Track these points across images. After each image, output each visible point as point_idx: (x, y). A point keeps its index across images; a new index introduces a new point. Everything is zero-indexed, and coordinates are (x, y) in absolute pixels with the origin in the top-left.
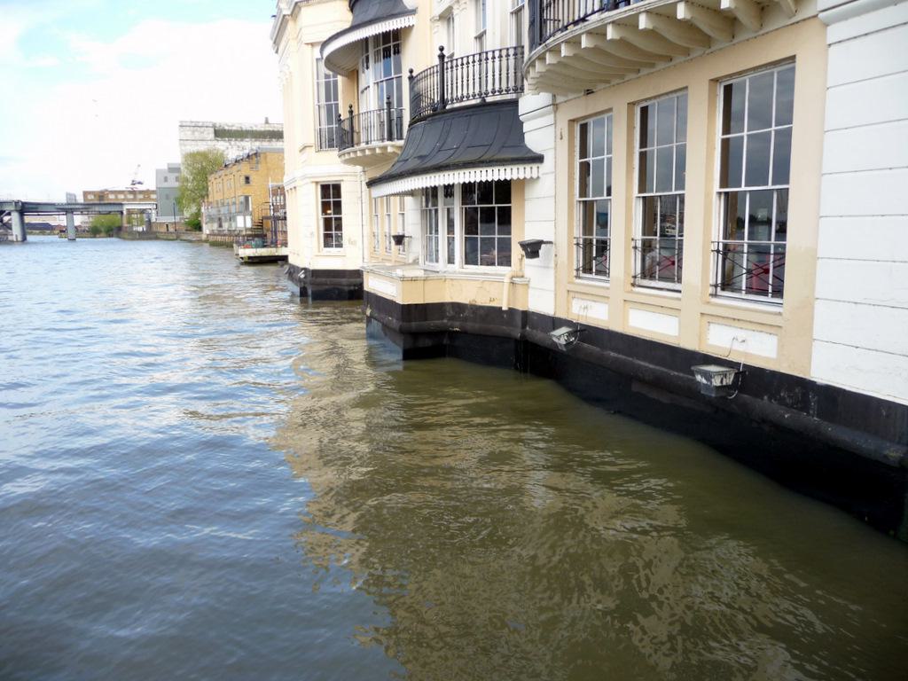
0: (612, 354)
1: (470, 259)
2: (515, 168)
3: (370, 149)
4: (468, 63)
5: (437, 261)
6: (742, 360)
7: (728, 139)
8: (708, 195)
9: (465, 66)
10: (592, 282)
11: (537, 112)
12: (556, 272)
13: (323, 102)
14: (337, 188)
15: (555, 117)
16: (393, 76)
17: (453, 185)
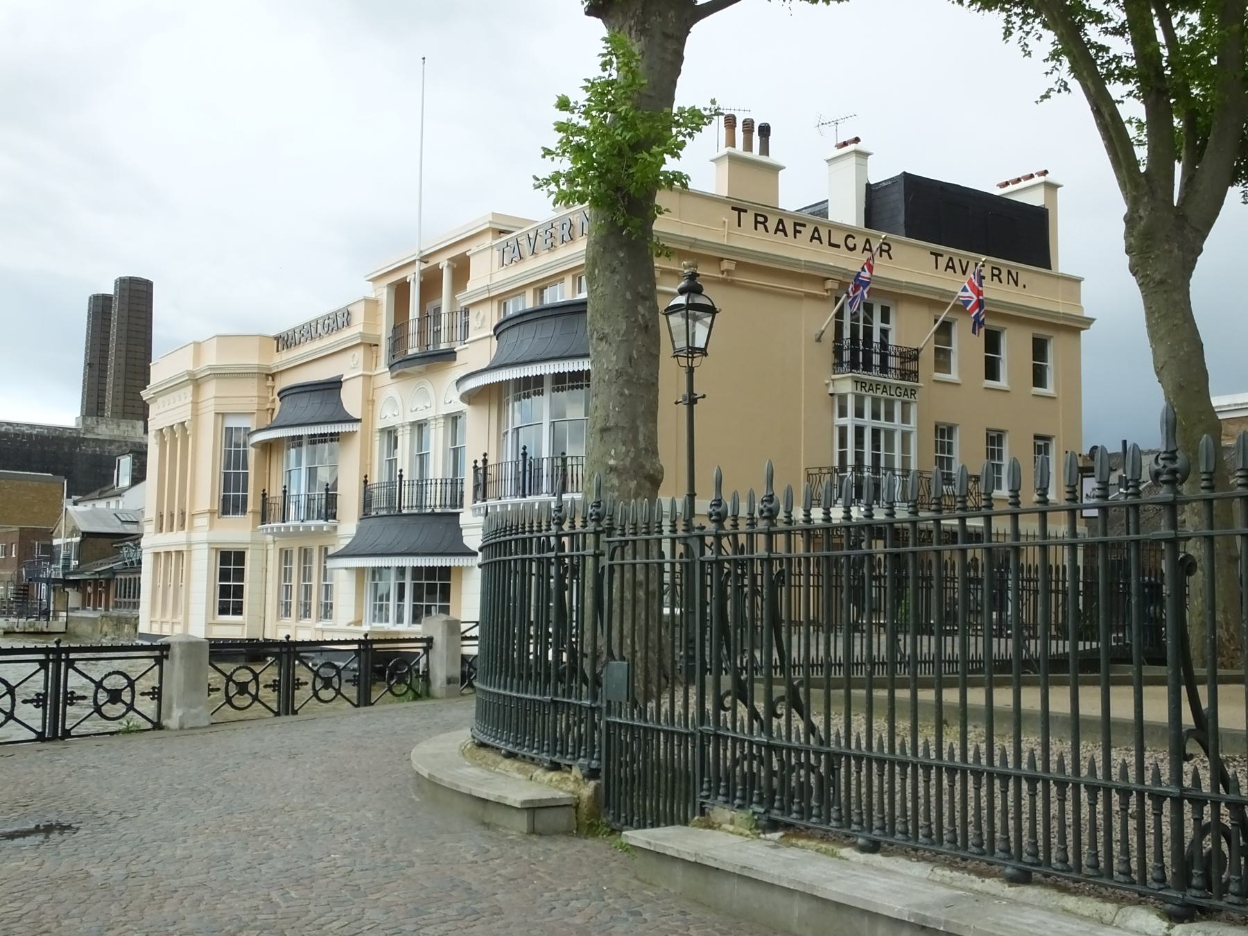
14: (240, 557)
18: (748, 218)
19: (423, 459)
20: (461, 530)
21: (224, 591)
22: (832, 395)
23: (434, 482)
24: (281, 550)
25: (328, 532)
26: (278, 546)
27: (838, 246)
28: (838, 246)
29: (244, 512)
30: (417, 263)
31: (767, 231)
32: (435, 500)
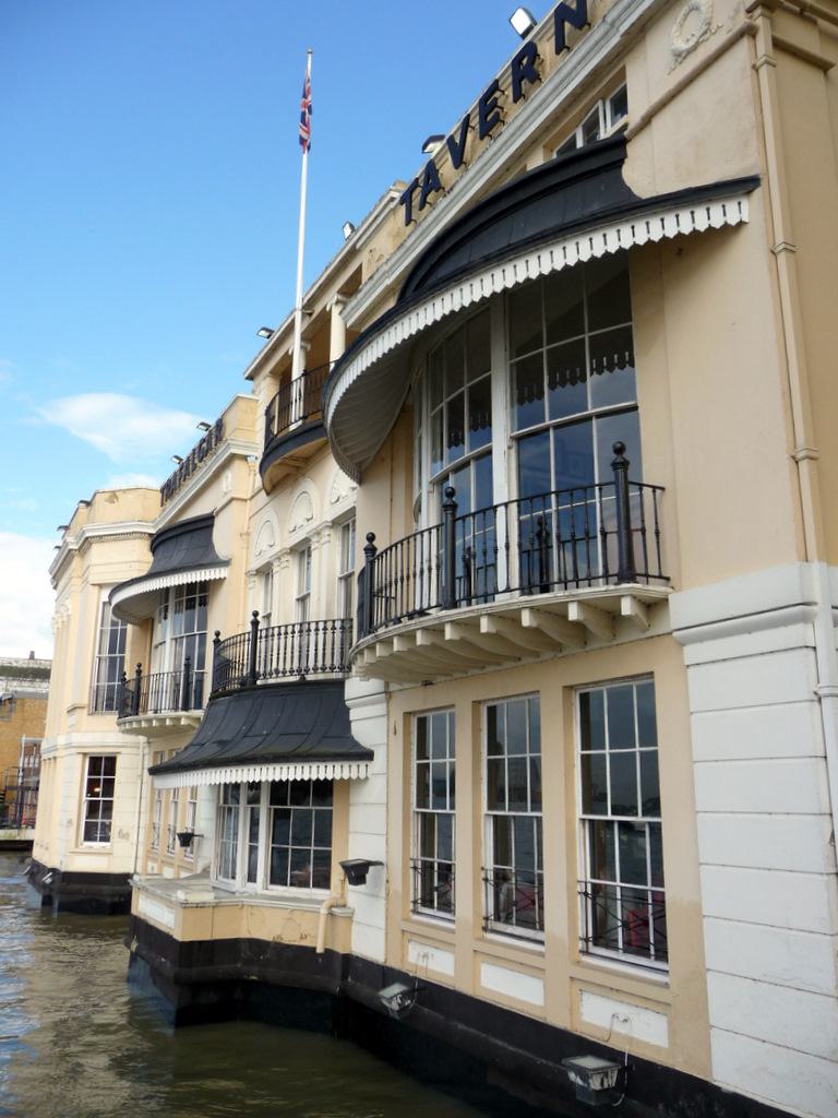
0: (461, 1026)
1: (277, 877)
2: (338, 765)
3: (158, 719)
4: (286, 633)
5: (234, 878)
6: (626, 1048)
7: (589, 755)
8: (569, 821)
9: (282, 637)
10: (432, 918)
11: (367, 698)
12: (387, 904)
13: (106, 654)
17: (260, 782)
20: (347, 710)
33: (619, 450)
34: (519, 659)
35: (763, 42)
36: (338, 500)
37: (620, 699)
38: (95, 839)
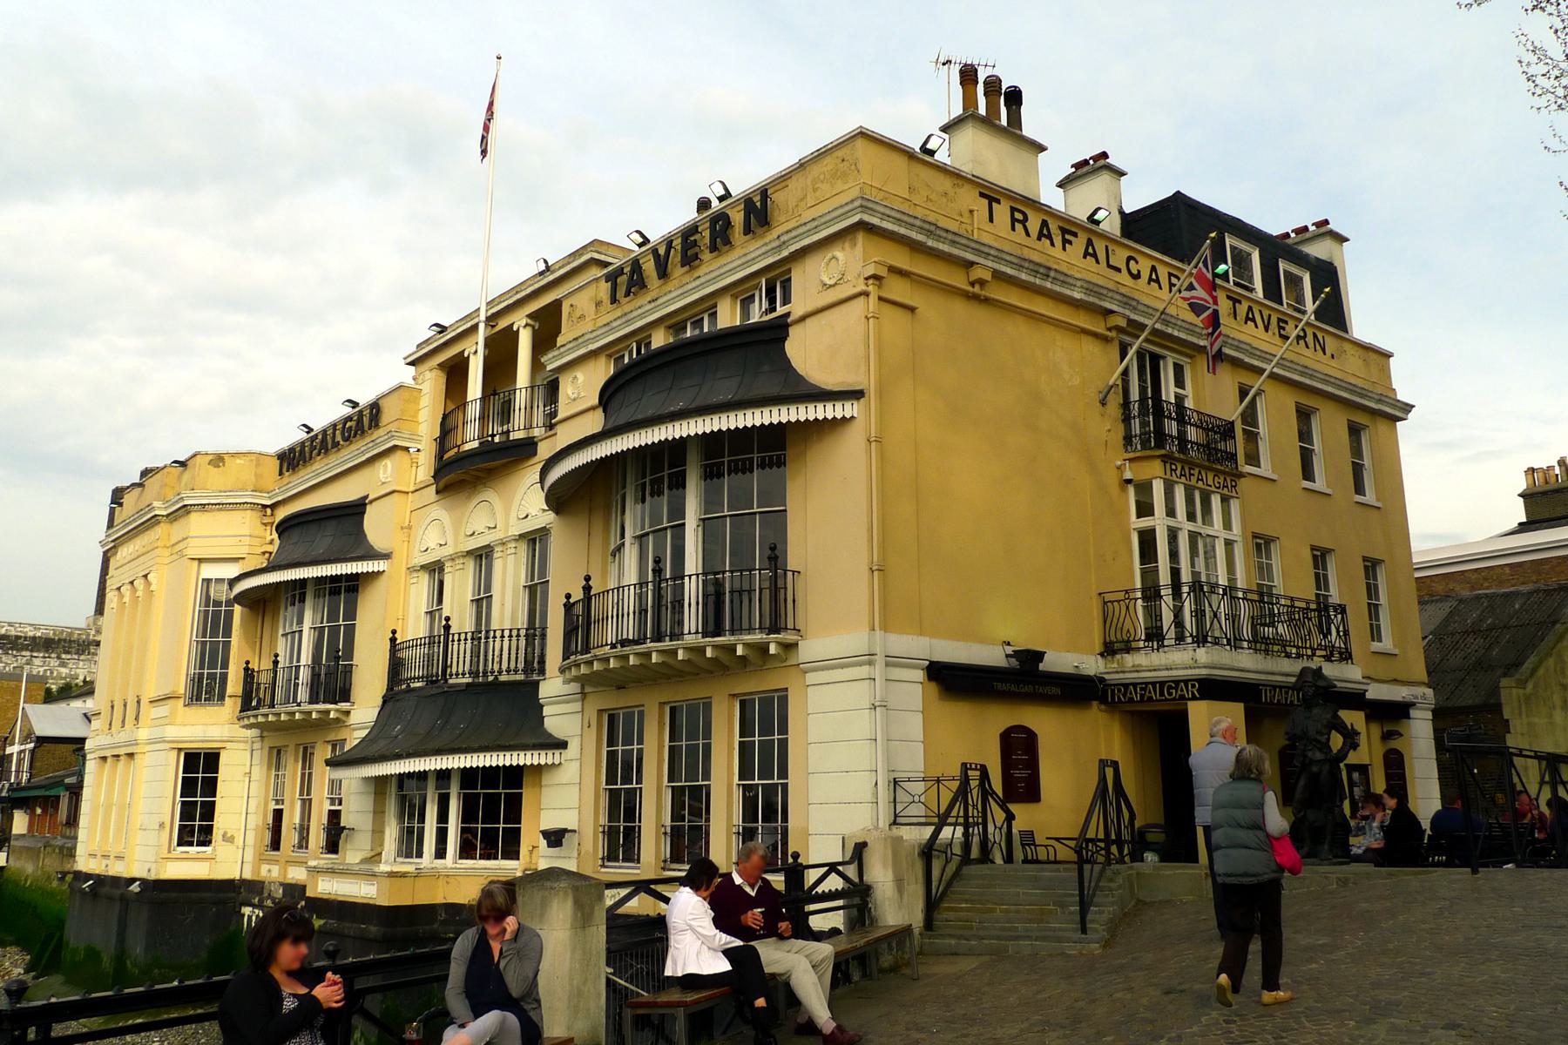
1: (466, 851)
15: (583, 705)
16: (341, 623)
18: (1002, 211)
19: (482, 603)
20: (542, 707)
21: (187, 811)
22: (1129, 481)
23: (498, 634)
24: (271, 748)
25: (337, 720)
26: (267, 743)
27: (1119, 270)
28: (1119, 270)
29: (222, 697)
30: (482, 326)
31: (1028, 234)
32: (505, 660)
33: (773, 548)
34: (698, 674)
35: (873, 299)
36: (527, 516)
37: (766, 703)
38: (191, 844)
